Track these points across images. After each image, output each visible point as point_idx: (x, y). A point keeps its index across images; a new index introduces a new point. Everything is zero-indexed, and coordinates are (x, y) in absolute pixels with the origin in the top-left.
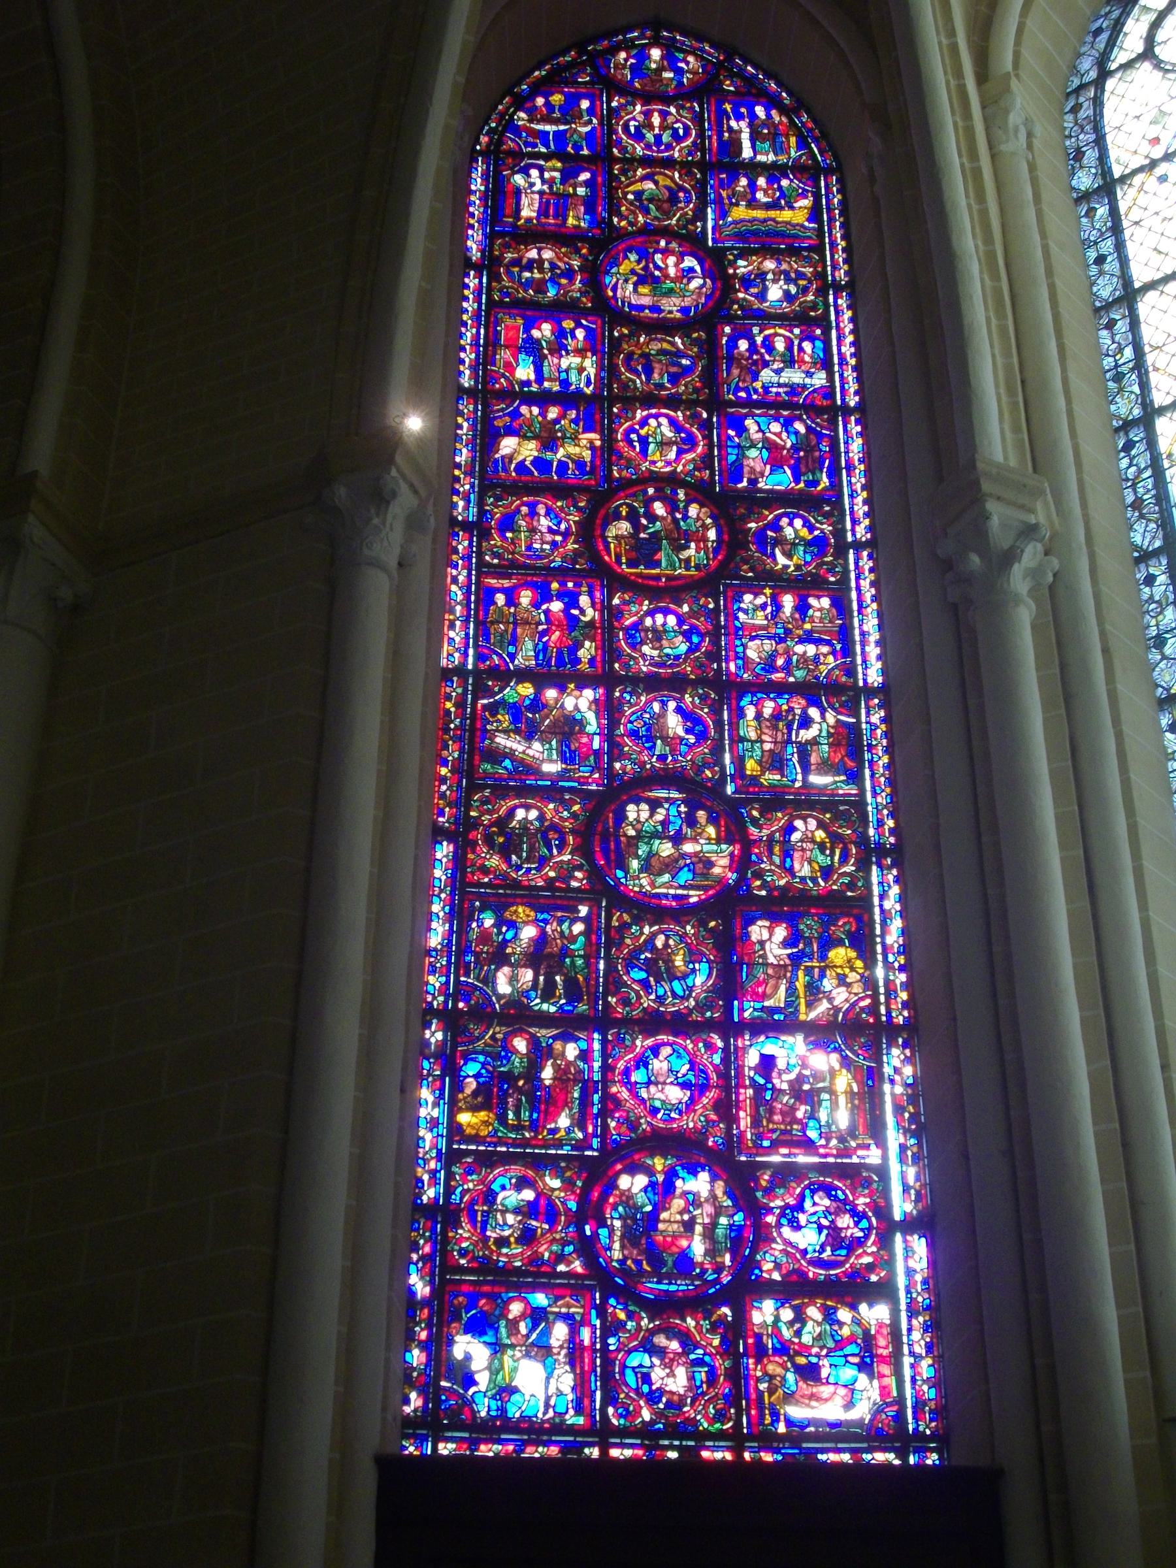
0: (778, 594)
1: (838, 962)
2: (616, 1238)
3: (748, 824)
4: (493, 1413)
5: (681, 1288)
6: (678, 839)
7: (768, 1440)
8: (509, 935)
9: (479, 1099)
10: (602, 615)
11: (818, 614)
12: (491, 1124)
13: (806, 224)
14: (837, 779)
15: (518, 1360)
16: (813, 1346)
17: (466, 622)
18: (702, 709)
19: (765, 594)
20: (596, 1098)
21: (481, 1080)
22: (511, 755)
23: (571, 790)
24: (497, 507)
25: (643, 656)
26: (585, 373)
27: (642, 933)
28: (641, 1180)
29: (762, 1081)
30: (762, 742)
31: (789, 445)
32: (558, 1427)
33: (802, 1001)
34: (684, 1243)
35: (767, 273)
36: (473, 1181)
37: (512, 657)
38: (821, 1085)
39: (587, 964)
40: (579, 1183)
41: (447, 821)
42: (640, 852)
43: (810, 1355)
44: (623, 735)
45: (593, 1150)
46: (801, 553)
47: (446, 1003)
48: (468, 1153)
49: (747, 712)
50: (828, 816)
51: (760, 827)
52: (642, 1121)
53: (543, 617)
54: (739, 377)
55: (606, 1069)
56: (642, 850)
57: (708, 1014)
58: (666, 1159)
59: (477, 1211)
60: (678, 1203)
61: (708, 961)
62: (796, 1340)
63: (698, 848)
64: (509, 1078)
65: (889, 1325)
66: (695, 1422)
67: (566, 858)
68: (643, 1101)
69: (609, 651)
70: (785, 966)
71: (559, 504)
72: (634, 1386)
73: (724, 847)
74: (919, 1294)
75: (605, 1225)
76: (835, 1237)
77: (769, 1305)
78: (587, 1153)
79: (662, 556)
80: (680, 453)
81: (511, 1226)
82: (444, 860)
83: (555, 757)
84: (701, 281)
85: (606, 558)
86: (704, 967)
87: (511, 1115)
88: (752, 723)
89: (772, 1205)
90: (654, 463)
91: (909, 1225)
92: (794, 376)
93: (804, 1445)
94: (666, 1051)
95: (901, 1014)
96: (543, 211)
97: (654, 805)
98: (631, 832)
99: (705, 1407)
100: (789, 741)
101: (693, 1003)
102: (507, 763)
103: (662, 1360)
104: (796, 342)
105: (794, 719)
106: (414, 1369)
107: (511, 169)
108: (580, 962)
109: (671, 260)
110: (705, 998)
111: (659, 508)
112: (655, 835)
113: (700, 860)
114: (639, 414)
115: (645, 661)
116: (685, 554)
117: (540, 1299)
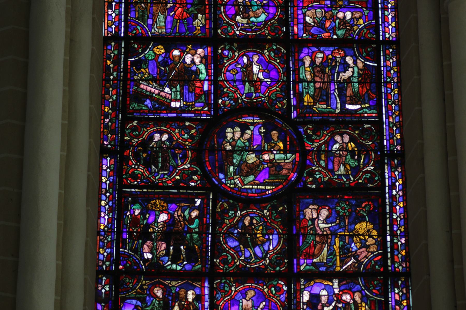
1: (361, 232)
3: (305, 140)
6: (259, 152)
8: (151, 219)
14: (363, 106)
18: (276, 61)
22: (150, 96)
23: (190, 120)
25: (237, 23)
27: (236, 216)
30: (315, 82)
33: (338, 258)
41: (110, 144)
42: (235, 161)
44: (223, 81)
47: (111, 265)
49: (306, 61)
50: (357, 132)
51: (313, 141)
56: (236, 159)
57: (278, 268)
61: (278, 234)
63: (272, 157)
67: (187, 166)
70: (327, 235)
73: (289, 155)
82: (108, 170)
83: (179, 97)
86: (275, 237)
88: (308, 69)
94: (251, 294)
95: (400, 265)
97: (244, 127)
98: (229, 148)
100: (333, 81)
101: (268, 261)
102: (148, 102)
105: (336, 65)
110: (276, 258)
112: (245, 149)
113: (274, 165)
115: (238, 27)
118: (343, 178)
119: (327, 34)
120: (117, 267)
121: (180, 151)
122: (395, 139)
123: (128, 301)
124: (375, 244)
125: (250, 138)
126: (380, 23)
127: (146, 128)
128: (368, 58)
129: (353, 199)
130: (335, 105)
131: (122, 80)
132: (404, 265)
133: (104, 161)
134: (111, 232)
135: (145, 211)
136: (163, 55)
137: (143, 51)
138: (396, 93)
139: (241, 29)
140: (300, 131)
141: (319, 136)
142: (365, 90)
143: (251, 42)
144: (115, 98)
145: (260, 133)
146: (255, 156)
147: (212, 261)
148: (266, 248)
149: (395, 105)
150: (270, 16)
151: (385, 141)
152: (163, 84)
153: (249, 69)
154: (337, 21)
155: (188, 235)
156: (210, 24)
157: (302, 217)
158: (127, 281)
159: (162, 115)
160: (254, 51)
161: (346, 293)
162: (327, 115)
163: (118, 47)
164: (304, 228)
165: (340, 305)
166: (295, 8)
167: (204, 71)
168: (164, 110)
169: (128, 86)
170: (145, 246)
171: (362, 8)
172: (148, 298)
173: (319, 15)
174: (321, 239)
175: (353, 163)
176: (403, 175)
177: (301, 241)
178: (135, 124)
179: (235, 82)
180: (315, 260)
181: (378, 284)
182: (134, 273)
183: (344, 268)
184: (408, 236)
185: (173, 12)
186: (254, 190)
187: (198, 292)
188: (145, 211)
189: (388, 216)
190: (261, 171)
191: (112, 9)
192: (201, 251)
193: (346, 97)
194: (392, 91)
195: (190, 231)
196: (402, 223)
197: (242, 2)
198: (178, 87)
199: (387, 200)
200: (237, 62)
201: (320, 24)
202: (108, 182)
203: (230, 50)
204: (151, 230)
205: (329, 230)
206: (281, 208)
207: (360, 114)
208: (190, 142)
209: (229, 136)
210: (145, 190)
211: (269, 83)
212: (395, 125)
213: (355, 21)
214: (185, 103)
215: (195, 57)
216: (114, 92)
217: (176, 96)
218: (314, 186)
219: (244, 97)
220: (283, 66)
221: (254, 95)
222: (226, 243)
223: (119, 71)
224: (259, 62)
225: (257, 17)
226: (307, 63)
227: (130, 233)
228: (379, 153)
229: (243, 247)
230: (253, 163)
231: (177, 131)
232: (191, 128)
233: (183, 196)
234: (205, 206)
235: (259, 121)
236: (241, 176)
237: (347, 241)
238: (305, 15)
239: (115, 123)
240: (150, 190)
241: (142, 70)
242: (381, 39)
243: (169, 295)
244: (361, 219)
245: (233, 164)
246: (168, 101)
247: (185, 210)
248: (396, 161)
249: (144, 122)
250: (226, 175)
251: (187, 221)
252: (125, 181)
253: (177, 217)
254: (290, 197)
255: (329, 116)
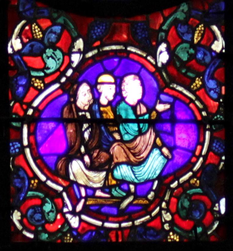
25: (71, 186)
139: (86, 210)
197: (90, 110)
225: (135, 162)
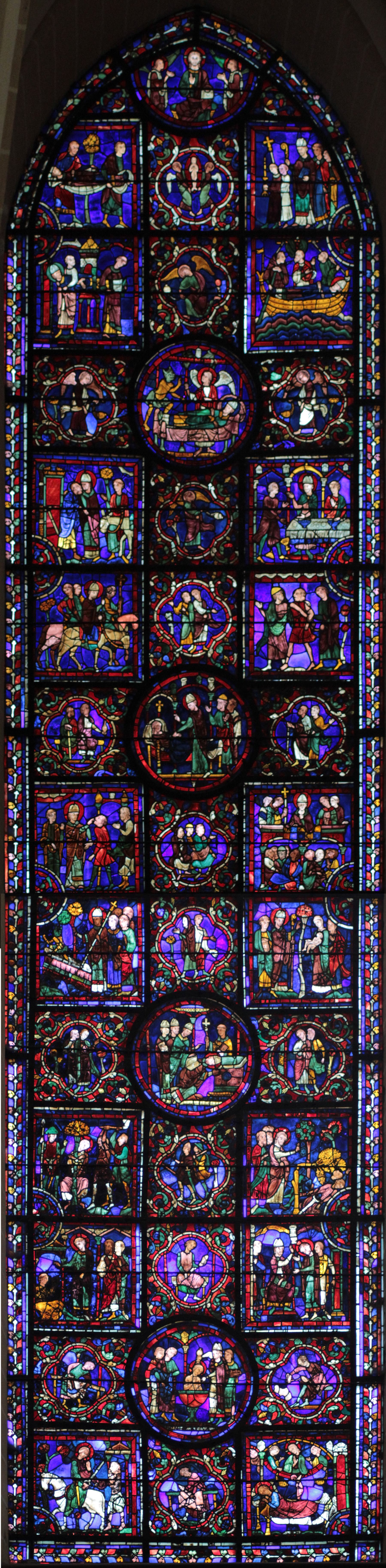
0: (294, 795)
2: (154, 1397)
3: (260, 1037)
4: (70, 1527)
5: (201, 1433)
6: (202, 1054)
7: (258, 1540)
8: (70, 1148)
9: (52, 1290)
10: (139, 828)
11: (327, 815)
12: (61, 1311)
13: (341, 315)
14: (334, 988)
15: (86, 1489)
16: (292, 1474)
17: (22, 845)
18: (224, 923)
19: (282, 795)
20: (138, 1286)
21: (52, 1275)
22: (64, 976)
23: (116, 1010)
24: (46, 709)
25: (175, 870)
26: (124, 537)
27: (173, 1142)
28: (172, 1351)
29: (263, 1268)
30: (274, 954)
31: (311, 617)
32: (114, 1535)
33: (297, 1197)
34: (202, 1399)
35: (299, 389)
36: (49, 1356)
37: (64, 877)
38: (308, 1269)
39: (130, 1173)
40: (126, 1355)
41: (16, 1045)
42: (172, 1067)
43: (290, 1480)
44: (157, 953)
45: (136, 1328)
46: (316, 746)
47: (22, 1209)
48: (45, 1334)
49: (262, 923)
52: (173, 1304)
53: (89, 833)
54: (268, 532)
55: (146, 1261)
56: (173, 1065)
58: (190, 1334)
59: (53, 1379)
60: (199, 1368)
61: (225, 1166)
62: (280, 1469)
63: (218, 1061)
64: (73, 1271)
65: (347, 1456)
66: (208, 1530)
67: (112, 1075)
68: (173, 1288)
69: (147, 867)
70: (285, 1167)
71: (101, 702)
72: (167, 1505)
73: (239, 1058)
74: (370, 1433)
75: (145, 1387)
76: (312, 1391)
77: (262, 1445)
78: (132, 1331)
79: (193, 758)
80: (211, 635)
81: (78, 1390)
82: (16, 1081)
83: (101, 978)
84: (234, 405)
85: (144, 763)
87: (75, 1303)
88: (265, 935)
89: (267, 1367)
90: (186, 647)
91: (367, 1380)
92: (320, 527)
93: (283, 1544)
94: (191, 1245)
95: (372, 1206)
96: (80, 317)
97: (184, 1019)
98: (165, 1048)
99: (216, 1519)
101: (212, 1203)
103: (185, 1487)
104: (324, 482)
105: (301, 929)
106: (15, 1498)
107: (47, 256)
108: (124, 1170)
109: (207, 376)
110: (221, 1198)
111: (191, 702)
113: (220, 1073)
114: (174, 586)
115: (177, 876)
116: (213, 754)
117: (100, 1445)
118: (306, 1089)
119: (291, 884)
120: (30, 1211)
121: (104, 1054)
122: (372, 1034)
123: (44, 1255)
124: (342, 1178)
125: (191, 1034)
126: (361, 866)
127: (61, 1022)
128: (342, 917)
129: (317, 1118)
130: (298, 987)
131: (30, 954)
132: (376, 1206)
133: (10, 1069)
134: (21, 1165)
135: (62, 1137)
136: (81, 917)
137: (56, 910)
138: (376, 968)
140: (253, 1025)
141: (277, 1031)
142: (337, 964)
143: (193, 897)
144: (21, 980)
145: (203, 1026)
146: (197, 1057)
147: (144, 1202)
148: (210, 1186)
149: (375, 985)
150: (219, 859)
151: (360, 1037)
152: (81, 959)
153: (190, 936)
154: (305, 864)
155: (115, 1169)
156: (141, 872)
157: (254, 1143)
158: (43, 1229)
159: (80, 1003)
160: (197, 910)
161: (305, 1243)
162: (288, 1001)
163: (23, 906)
164: (256, 1158)
165: (297, 1259)
166: (252, 846)
167: (133, 940)
168: (83, 996)
169: (37, 963)
170: (63, 1183)
171: (337, 844)
172: (68, 1252)
173: (282, 855)
174: (276, 1173)
175: (319, 1069)
176: (380, 1085)
177: (252, 1176)
178: (47, 1017)
179: (172, 954)
180: (268, 1201)
181: (344, 1231)
182: (49, 1218)
183: (304, 1210)
184: (382, 1167)
185: (93, 856)
186: (195, 1108)
187: (128, 1244)
188: (62, 1137)
189: (359, 1141)
190: (204, 1081)
191: (13, 853)
192: (131, 1189)
193: (313, 975)
194: (371, 965)
195: (117, 1163)
196: (377, 1150)
198: (100, 963)
199: (359, 1120)
200: (174, 925)
201: (283, 869)
202: (16, 1098)
203: (166, 907)
204: (69, 1162)
205: (287, 1160)
206: (228, 1131)
207: (330, 999)
208: (116, 1042)
209: (165, 1031)
210: (61, 1109)
211: (215, 955)
212: (372, 1014)
213: (329, 864)
214: (109, 986)
215: (121, 920)
216: (20, 971)
217: (97, 975)
218: (270, 1101)
219: (183, 976)
220: (233, 930)
221: (197, 973)
222: (161, 1179)
223: (25, 942)
224: (203, 925)
226: (265, 925)
227: (45, 1167)
228: (351, 1055)
229: (183, 1184)
230: (194, 1070)
231: (99, 1026)
232: (116, 1021)
233: (108, 1116)
234: (136, 1129)
235: (201, 1010)
236: (180, 1087)
237: (308, 1175)
238: (263, 856)
239: (22, 1015)
240: (67, 1109)
241: (55, 939)
242: (361, 889)
243: (93, 1247)
244: (326, 1145)
245: (169, 1071)
246: (88, 983)
247: (111, 1135)
248: (372, 1065)
249: (59, 1014)
250: (161, 1086)
251: (114, 1149)
252: (36, 1095)
253: (101, 1145)
254: (240, 1115)
255: (290, 1003)
